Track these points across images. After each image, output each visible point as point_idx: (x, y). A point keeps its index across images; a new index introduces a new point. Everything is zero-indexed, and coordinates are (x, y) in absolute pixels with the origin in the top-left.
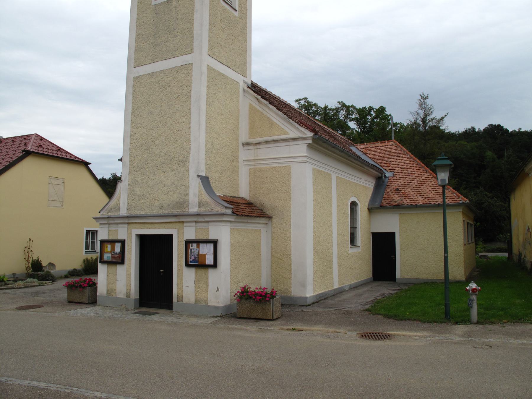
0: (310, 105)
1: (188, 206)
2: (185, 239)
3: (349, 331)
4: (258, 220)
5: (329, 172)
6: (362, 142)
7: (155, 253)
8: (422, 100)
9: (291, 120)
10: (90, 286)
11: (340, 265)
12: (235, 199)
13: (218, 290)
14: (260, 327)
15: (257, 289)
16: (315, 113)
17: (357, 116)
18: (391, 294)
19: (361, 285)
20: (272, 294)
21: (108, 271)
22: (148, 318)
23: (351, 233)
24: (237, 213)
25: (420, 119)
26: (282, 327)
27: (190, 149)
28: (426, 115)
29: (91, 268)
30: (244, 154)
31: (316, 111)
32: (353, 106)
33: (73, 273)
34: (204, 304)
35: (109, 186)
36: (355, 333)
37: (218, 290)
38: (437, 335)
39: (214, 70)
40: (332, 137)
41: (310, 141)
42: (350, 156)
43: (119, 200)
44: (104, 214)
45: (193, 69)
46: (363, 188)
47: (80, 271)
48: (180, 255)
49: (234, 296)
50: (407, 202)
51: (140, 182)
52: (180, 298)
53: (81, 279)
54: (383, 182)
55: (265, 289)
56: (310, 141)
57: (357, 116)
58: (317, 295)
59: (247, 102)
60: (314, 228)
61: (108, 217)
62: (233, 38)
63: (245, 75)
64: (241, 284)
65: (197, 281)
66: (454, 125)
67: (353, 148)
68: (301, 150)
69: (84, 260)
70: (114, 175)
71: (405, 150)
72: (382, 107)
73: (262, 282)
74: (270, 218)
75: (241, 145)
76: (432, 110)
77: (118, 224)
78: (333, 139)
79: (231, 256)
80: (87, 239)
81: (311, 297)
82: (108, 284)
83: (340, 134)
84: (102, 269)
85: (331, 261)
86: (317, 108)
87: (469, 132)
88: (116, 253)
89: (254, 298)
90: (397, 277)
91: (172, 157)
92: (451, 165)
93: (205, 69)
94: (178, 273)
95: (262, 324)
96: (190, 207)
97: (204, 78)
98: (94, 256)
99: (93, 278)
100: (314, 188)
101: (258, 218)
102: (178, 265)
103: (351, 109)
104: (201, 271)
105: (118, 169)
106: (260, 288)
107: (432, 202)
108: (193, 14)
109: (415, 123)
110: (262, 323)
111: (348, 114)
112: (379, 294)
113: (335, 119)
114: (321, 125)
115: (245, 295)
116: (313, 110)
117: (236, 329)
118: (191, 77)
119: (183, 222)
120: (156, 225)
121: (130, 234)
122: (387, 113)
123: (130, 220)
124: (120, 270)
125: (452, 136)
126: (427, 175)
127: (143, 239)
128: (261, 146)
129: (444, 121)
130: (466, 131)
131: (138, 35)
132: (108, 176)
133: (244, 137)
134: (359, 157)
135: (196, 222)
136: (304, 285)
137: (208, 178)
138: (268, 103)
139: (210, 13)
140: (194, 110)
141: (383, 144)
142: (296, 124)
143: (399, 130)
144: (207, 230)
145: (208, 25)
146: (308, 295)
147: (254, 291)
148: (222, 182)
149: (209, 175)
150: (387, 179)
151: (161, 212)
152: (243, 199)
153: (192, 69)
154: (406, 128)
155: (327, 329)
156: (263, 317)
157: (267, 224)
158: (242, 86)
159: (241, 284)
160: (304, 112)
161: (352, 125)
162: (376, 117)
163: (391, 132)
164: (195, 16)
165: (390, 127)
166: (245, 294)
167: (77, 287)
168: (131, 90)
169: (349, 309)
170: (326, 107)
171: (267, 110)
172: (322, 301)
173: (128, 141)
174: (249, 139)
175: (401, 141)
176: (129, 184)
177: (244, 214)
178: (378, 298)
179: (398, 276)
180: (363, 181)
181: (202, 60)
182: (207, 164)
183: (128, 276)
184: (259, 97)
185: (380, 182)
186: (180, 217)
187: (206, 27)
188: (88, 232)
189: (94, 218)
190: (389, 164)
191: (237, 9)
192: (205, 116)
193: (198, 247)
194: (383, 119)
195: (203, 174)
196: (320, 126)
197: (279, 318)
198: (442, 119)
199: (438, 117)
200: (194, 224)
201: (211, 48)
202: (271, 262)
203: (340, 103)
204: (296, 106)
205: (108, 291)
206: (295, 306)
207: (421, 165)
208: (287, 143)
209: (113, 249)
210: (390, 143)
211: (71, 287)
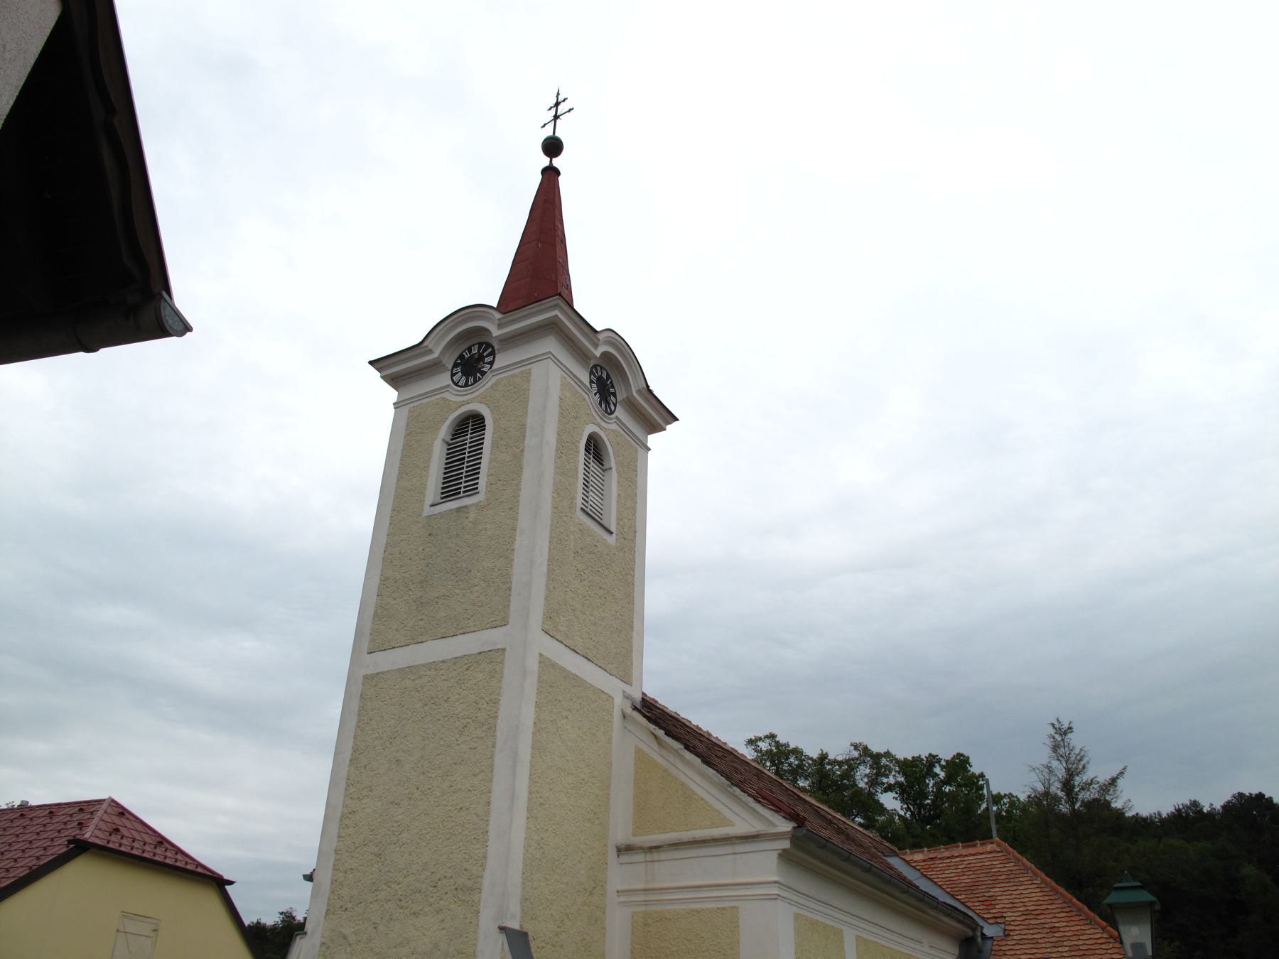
6: (916, 846)
8: (1058, 738)
9: (738, 791)
16: (797, 772)
17: (901, 779)
25: (1058, 785)
27: (485, 857)
28: (1071, 774)
30: (620, 876)
32: (887, 754)
39: (554, 665)
40: (840, 831)
41: (786, 844)
42: (888, 882)
54: (980, 951)
56: (786, 844)
57: (901, 779)
62: (601, 592)
63: (626, 678)
66: (1147, 797)
67: (894, 861)
68: (763, 865)
70: (288, 917)
71: (1028, 864)
72: (959, 755)
75: (612, 853)
78: (842, 837)
83: (860, 824)
86: (802, 761)
87: (1188, 814)
91: (438, 876)
93: (533, 664)
97: (531, 685)
103: (884, 761)
108: (512, 540)
109: (1047, 794)
111: (878, 774)
113: (846, 788)
114: (813, 801)
116: (790, 765)
118: (500, 681)
125: (1142, 825)
128: (663, 855)
130: (1179, 810)
131: (384, 580)
132: (271, 918)
133: (621, 831)
134: (911, 884)
137: (526, 934)
139: (551, 537)
140: (501, 760)
141: (971, 850)
142: (750, 800)
143: (1007, 811)
145: (546, 563)
148: (562, 946)
149: (529, 928)
150: (989, 942)
153: (502, 662)
154: (1024, 808)
160: (768, 769)
161: (890, 801)
162: (947, 781)
163: (988, 818)
164: (517, 543)
165: (984, 806)
168: (355, 705)
170: (823, 757)
173: (334, 829)
174: (634, 835)
175: (1015, 840)
180: (926, 949)
181: (529, 642)
182: (525, 899)
184: (661, 733)
190: (989, 902)
191: (613, 529)
194: (965, 786)
195: (515, 925)
196: (810, 804)
198: (1113, 781)
199: (1103, 777)
201: (549, 615)
203: (856, 747)
204: (749, 754)
207: (1074, 905)
208: (729, 849)
210: (989, 847)
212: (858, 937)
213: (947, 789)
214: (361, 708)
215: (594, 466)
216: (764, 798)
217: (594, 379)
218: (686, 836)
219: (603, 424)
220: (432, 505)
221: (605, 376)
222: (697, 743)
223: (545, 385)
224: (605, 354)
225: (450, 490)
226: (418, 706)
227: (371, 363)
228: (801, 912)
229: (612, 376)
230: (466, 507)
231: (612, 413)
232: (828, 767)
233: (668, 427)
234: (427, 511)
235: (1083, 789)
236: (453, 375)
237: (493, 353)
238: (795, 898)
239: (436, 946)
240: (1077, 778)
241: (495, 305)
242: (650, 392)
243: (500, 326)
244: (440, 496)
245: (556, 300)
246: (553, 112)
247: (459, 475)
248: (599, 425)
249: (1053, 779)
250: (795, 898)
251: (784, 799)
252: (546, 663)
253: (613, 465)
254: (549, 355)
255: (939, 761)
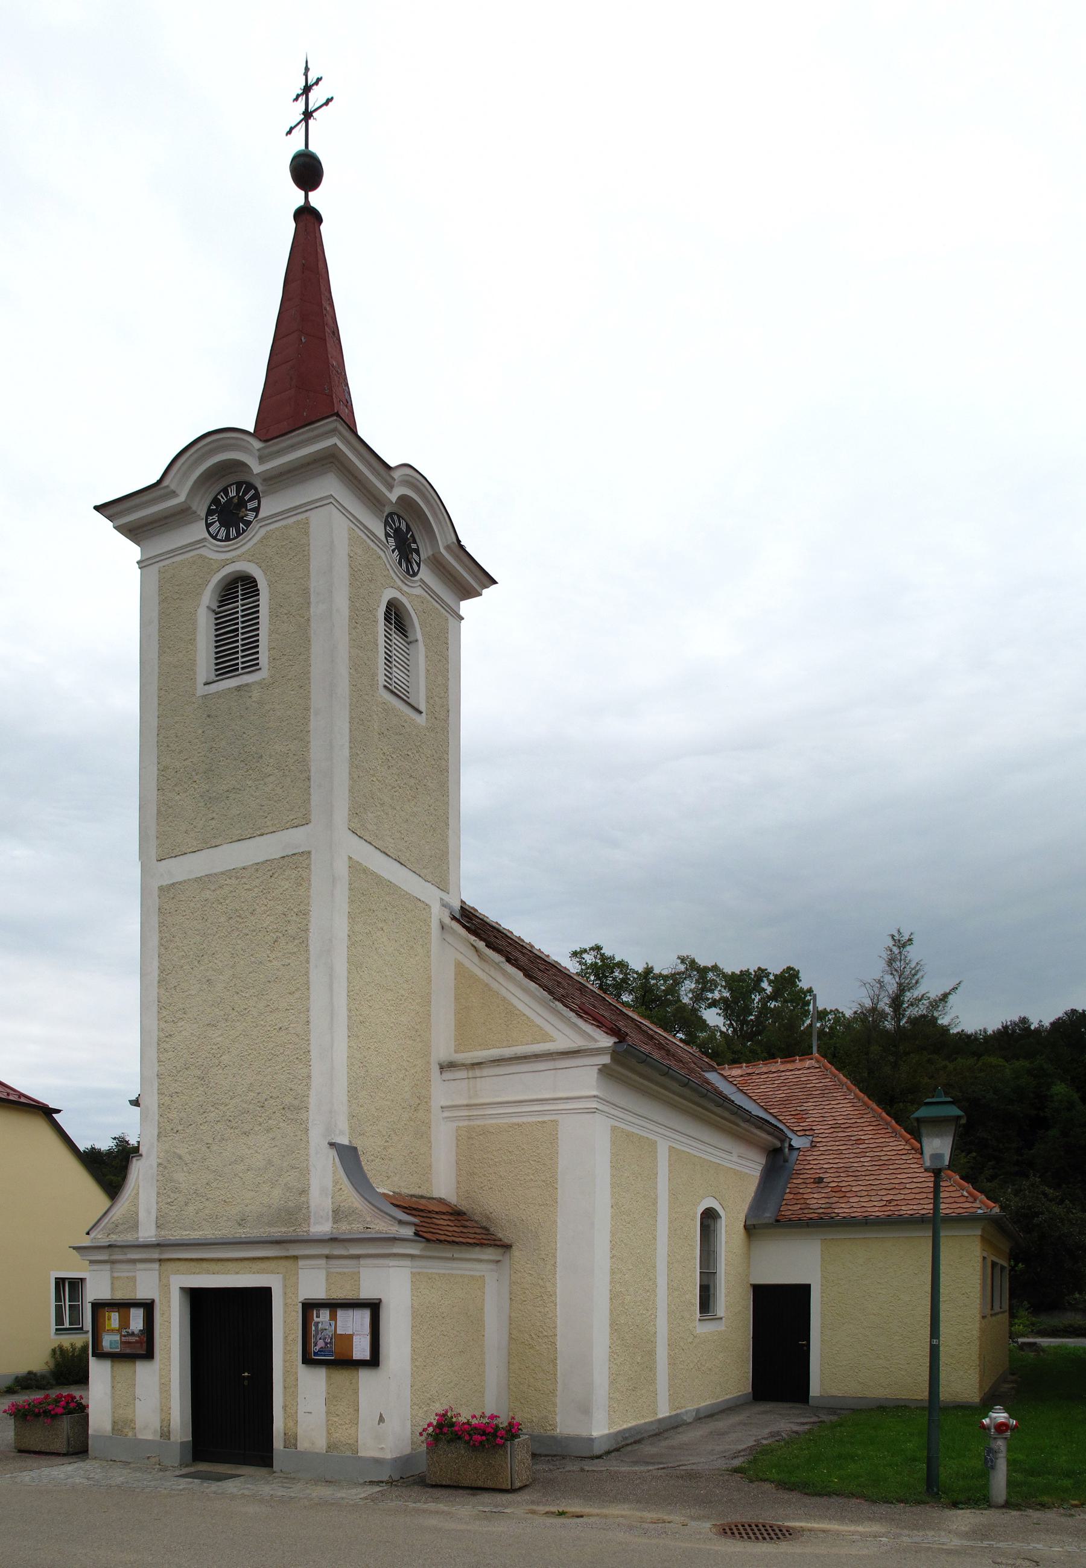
0: (608, 966)
1: (307, 1219)
2: (301, 1298)
3: (693, 1518)
4: (477, 1253)
5: (651, 1136)
6: (735, 1062)
7: (230, 1335)
8: (896, 950)
9: (559, 1006)
10: (70, 1413)
11: (672, 1362)
12: (423, 1201)
13: (381, 1419)
14: (481, 1508)
15: (474, 1417)
16: (621, 986)
17: (726, 994)
18: (796, 1432)
19: (722, 1411)
20: (510, 1430)
21: (113, 1377)
22: (214, 1487)
23: (701, 1286)
24: (425, 1235)
25: (887, 1000)
26: (535, 1507)
27: (309, 1077)
28: (902, 989)
29: (70, 1370)
30: (444, 1092)
31: (622, 980)
32: (715, 968)
33: (27, 1382)
34: (348, 1453)
35: (110, 1168)
36: (708, 1525)
37: (381, 1419)
38: (906, 1532)
39: (365, 870)
40: (660, 1047)
41: (606, 1059)
42: (704, 1096)
43: (136, 1205)
44: (100, 1237)
45: (313, 867)
46: (732, 1175)
47: (43, 1377)
48: (290, 1338)
49: (421, 1434)
50: (843, 1210)
51: (188, 1158)
52: (291, 1441)
53: (47, 1396)
54: (786, 1161)
55: (492, 1417)
56: (606, 1059)
57: (726, 994)
58: (619, 1432)
59: (451, 955)
60: (613, 1273)
61: (110, 1246)
62: (412, 782)
63: (443, 884)
64: (437, 1405)
65: (331, 1399)
66: (973, 1015)
67: (712, 1077)
68: (584, 1080)
69: (54, 1351)
70: (122, 1142)
71: (845, 1080)
72: (789, 968)
73: (486, 1400)
74: (507, 1247)
75: (435, 1069)
76: (920, 974)
77: (134, 1261)
78: (663, 1053)
79: (413, 1340)
80: (58, 1298)
81: (602, 1437)
82: (115, 1407)
83: (681, 1040)
84: (99, 1372)
85: (651, 1353)
86: (626, 974)
87: (1014, 1031)
88: (133, 1334)
89: (467, 1438)
90: (811, 1394)
91: (264, 1096)
92: (958, 1117)
93: (342, 868)
94: (285, 1381)
95: (486, 1502)
96: (312, 1221)
98: (78, 1340)
99: (76, 1392)
100: (613, 1176)
101: (478, 1249)
102: (285, 1361)
103: (710, 975)
104: (342, 1376)
105: (130, 1126)
106: (483, 1416)
107: (906, 1210)
108: (306, 720)
109: (874, 1009)
110: (486, 1498)
111: (703, 990)
112: (767, 1431)
113: (669, 1003)
114: (636, 1017)
115: (446, 1432)
116: (614, 979)
117: (424, 1511)
118: (308, 889)
119: (296, 1258)
120: (230, 1265)
121: (165, 1288)
122: (803, 984)
123: (163, 1252)
124: (144, 1372)
125: (968, 1044)
126: (895, 1145)
127: (199, 1300)
128: (486, 1072)
129: (949, 1004)
130: (1006, 1028)
131: (163, 770)
132: (105, 1144)
133: (443, 1048)
134: (726, 1098)
135: (327, 1257)
136: (586, 1410)
137: (356, 1148)
138: (503, 959)
139: (351, 718)
140: (316, 976)
141: (790, 1066)
142: (572, 1014)
143: (831, 1028)
144: (356, 1277)
145: (347, 744)
146: (595, 1434)
147: (468, 1423)
148: (391, 1159)
149: (358, 1143)
150: (795, 1153)
151: (242, 1233)
152: (441, 1201)
153: (308, 867)
154: (848, 1024)
155: (639, 1514)
156: (489, 1484)
157: (498, 1261)
158: (438, 914)
159: (437, 1405)
160: (592, 983)
161: (713, 1017)
162: (773, 997)
163: (811, 1035)
164: (313, 725)
165: (808, 1022)
166: (445, 1430)
167: (38, 1415)
168: (154, 920)
169: (694, 1467)
170: (649, 971)
171: (501, 979)
172: (629, 1448)
173: (153, 1053)
174: (456, 1052)
175: (834, 1056)
176: (160, 1164)
177: (442, 1238)
178: (765, 1442)
179: (815, 1389)
180: (735, 1159)
181: (336, 847)
182: (352, 1116)
183: (164, 1388)
184: (481, 945)
185: (777, 1160)
186: (288, 1245)
187: (343, 752)
188: (60, 1282)
189: (74, 1248)
190: (800, 1117)
191: (422, 708)
192: (344, 993)
193: (333, 1317)
194: (792, 1001)
195: (345, 1141)
196: (633, 1020)
197: (526, 1486)
198: (945, 997)
199: (935, 993)
200: (323, 1262)
201: (356, 811)
202: (509, 1354)
203: (683, 960)
204: (572, 967)
205: (114, 1423)
206: (564, 1457)
207: (883, 1119)
208: (550, 1065)
209: (125, 1322)
210: (808, 1063)
211: (22, 1415)
212: (671, 1148)
213: (772, 1005)
214: (161, 924)
215: (396, 638)
216: (586, 1013)
217: (391, 532)
218: (508, 1052)
219: (405, 588)
220: (206, 684)
221: (404, 527)
222: (520, 956)
223: (327, 539)
224: (403, 499)
225: (225, 667)
226: (222, 920)
227: (97, 508)
228: (616, 1124)
229: (411, 522)
230: (247, 685)
231: (415, 574)
232: (653, 982)
233: (485, 591)
234: (201, 690)
235: (912, 1005)
236: (208, 526)
237: (256, 497)
238: (613, 1112)
239: (270, 1162)
240: (908, 994)
241: (252, 431)
242: (462, 547)
243: (262, 459)
244: (213, 673)
245: (332, 423)
246: (301, 105)
247: (234, 649)
248: (400, 590)
249: (883, 994)
250: (613, 1112)
251: (606, 1014)
252: (356, 868)
253: (419, 636)
254: (328, 500)
255: (767, 975)
